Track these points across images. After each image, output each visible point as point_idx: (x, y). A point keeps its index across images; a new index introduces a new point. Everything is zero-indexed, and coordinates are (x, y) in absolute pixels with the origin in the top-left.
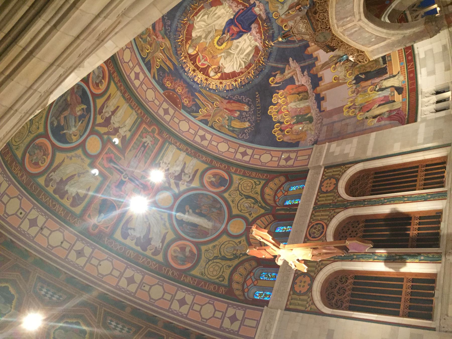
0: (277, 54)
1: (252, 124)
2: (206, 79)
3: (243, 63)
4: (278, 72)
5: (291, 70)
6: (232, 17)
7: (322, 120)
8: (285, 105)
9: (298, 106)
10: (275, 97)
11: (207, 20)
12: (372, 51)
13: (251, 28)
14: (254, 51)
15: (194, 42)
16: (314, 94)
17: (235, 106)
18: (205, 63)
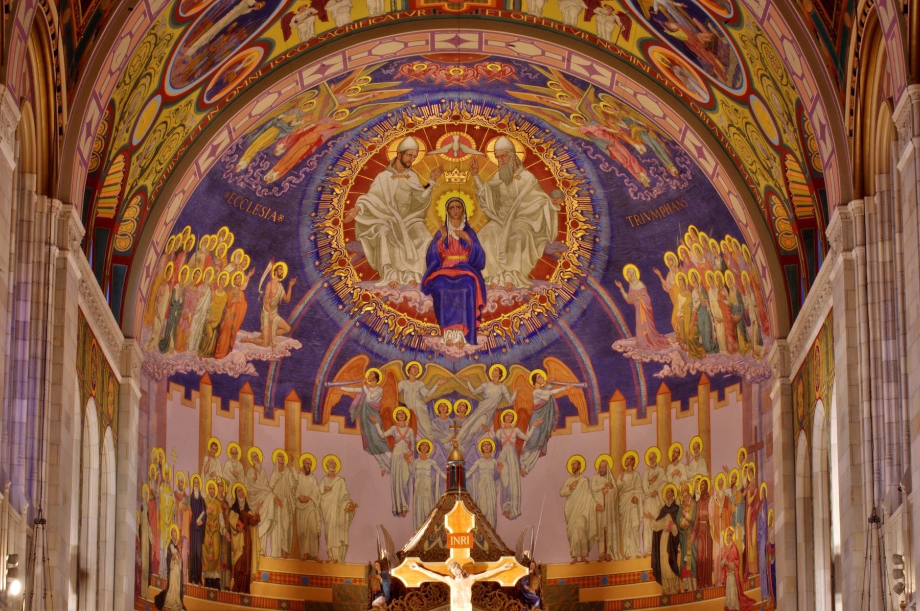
0: (328, 316)
2: (411, 126)
5: (274, 334)
6: (485, 273)
8: (215, 279)
9: (196, 316)
10: (245, 260)
11: (529, 221)
13: (426, 294)
14: (373, 266)
16: (201, 373)
17: (300, 150)
18: (446, 148)
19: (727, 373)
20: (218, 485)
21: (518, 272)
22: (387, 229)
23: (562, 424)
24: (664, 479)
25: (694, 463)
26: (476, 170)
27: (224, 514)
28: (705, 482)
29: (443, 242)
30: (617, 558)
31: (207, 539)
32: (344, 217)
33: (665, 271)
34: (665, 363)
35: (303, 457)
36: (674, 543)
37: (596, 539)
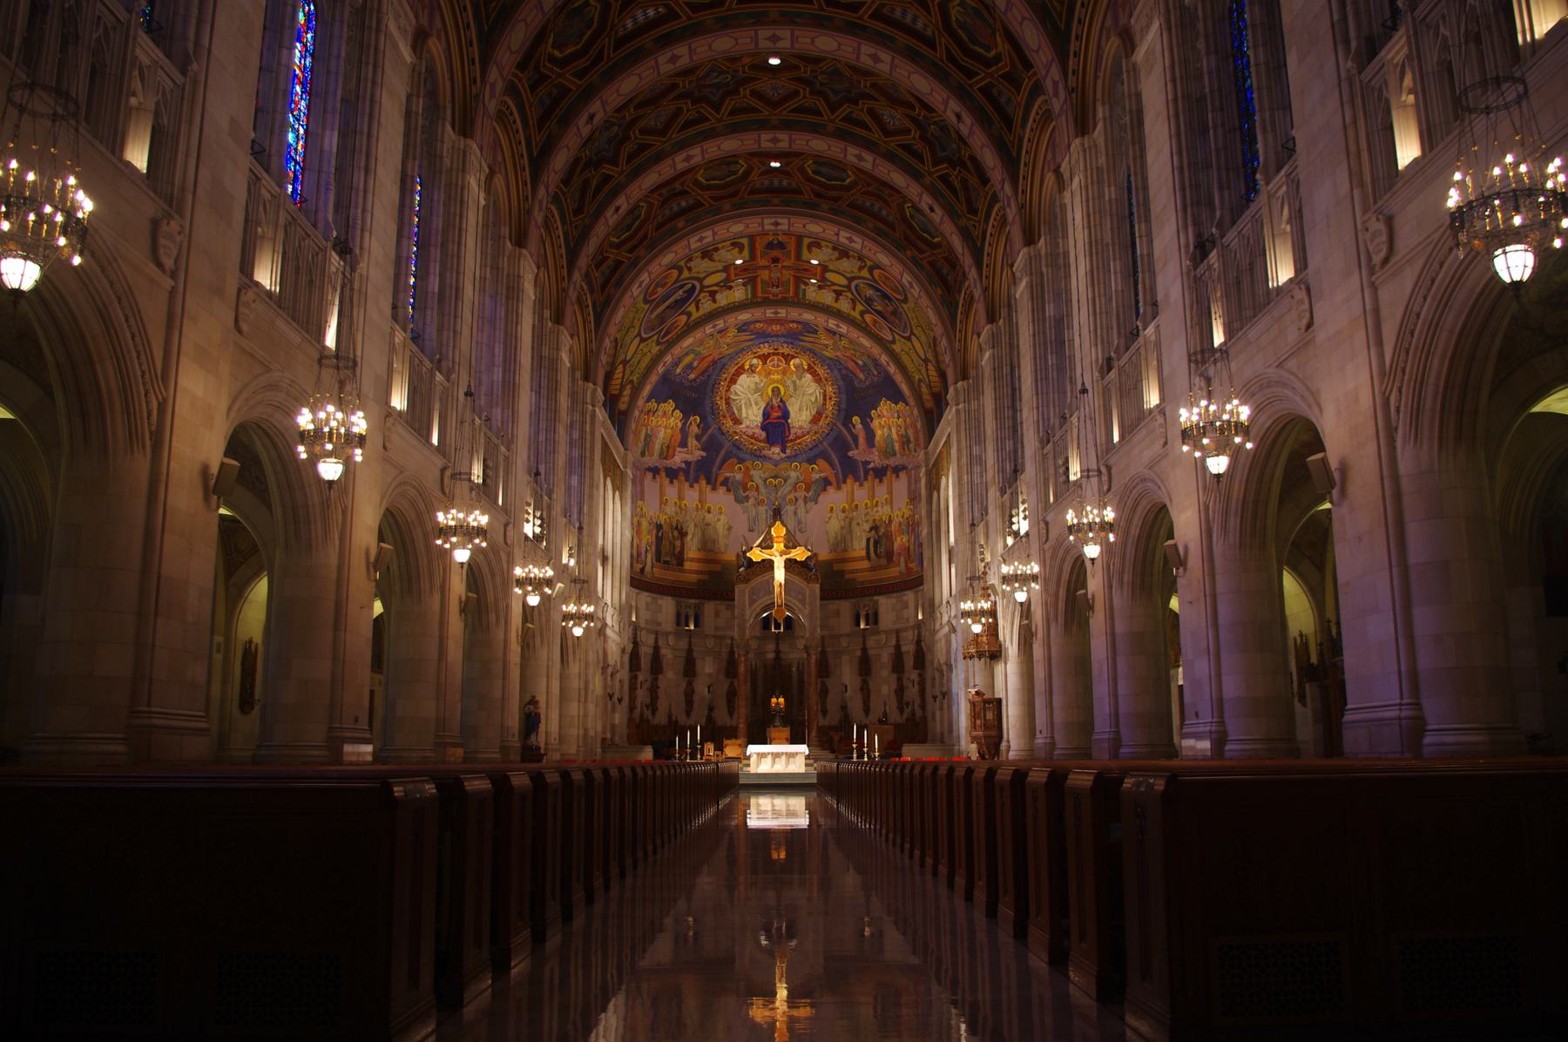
17: (705, 364)
23: (825, 490)
33: (872, 419)
36: (876, 543)
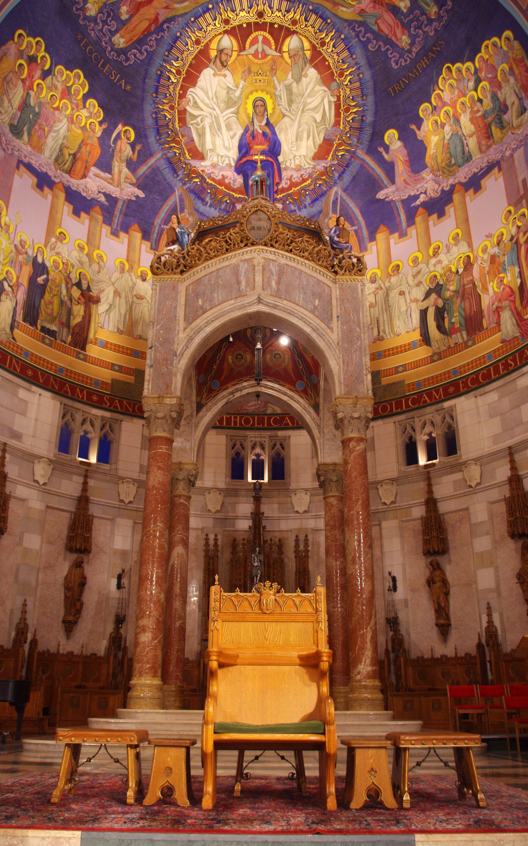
0: (166, 180)
1: (85, 18)
2: (227, 22)
3: (195, 112)
4: (135, 158)
5: (122, 180)
6: (280, 158)
7: (4, 150)
9: (52, 134)
10: (98, 111)
11: (313, 114)
12: (174, 288)
13: (238, 174)
14: (200, 149)
15: (300, 62)
18: (253, 50)
19: (481, 169)
20: (63, 263)
21: (304, 156)
22: (210, 121)
24: (427, 270)
25: (454, 249)
26: (274, 71)
27: (67, 286)
28: (468, 257)
29: (251, 135)
30: (389, 337)
31: (47, 296)
32: (178, 105)
33: (419, 122)
34: (421, 193)
35: (141, 269)
36: (440, 314)
37: (371, 327)
